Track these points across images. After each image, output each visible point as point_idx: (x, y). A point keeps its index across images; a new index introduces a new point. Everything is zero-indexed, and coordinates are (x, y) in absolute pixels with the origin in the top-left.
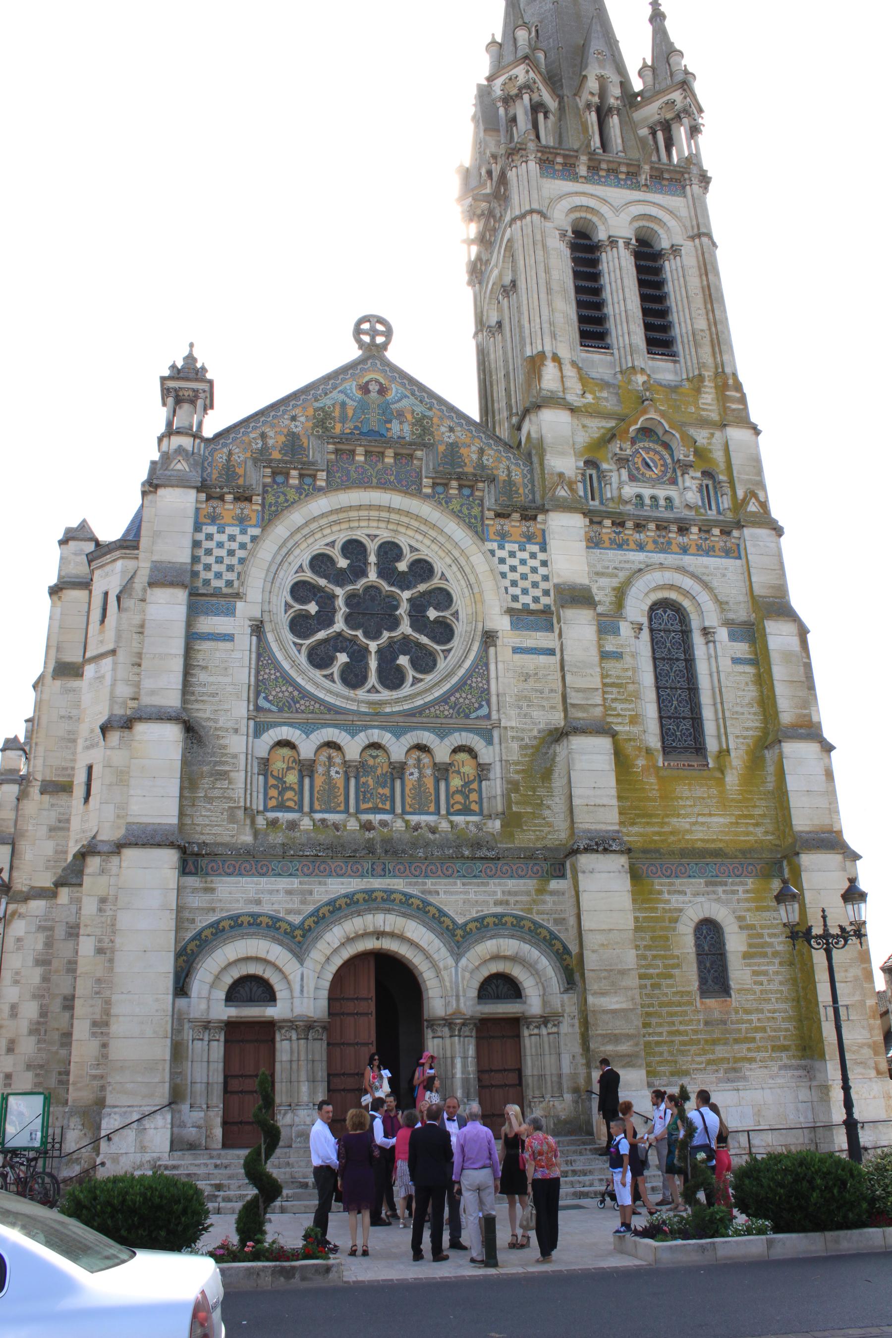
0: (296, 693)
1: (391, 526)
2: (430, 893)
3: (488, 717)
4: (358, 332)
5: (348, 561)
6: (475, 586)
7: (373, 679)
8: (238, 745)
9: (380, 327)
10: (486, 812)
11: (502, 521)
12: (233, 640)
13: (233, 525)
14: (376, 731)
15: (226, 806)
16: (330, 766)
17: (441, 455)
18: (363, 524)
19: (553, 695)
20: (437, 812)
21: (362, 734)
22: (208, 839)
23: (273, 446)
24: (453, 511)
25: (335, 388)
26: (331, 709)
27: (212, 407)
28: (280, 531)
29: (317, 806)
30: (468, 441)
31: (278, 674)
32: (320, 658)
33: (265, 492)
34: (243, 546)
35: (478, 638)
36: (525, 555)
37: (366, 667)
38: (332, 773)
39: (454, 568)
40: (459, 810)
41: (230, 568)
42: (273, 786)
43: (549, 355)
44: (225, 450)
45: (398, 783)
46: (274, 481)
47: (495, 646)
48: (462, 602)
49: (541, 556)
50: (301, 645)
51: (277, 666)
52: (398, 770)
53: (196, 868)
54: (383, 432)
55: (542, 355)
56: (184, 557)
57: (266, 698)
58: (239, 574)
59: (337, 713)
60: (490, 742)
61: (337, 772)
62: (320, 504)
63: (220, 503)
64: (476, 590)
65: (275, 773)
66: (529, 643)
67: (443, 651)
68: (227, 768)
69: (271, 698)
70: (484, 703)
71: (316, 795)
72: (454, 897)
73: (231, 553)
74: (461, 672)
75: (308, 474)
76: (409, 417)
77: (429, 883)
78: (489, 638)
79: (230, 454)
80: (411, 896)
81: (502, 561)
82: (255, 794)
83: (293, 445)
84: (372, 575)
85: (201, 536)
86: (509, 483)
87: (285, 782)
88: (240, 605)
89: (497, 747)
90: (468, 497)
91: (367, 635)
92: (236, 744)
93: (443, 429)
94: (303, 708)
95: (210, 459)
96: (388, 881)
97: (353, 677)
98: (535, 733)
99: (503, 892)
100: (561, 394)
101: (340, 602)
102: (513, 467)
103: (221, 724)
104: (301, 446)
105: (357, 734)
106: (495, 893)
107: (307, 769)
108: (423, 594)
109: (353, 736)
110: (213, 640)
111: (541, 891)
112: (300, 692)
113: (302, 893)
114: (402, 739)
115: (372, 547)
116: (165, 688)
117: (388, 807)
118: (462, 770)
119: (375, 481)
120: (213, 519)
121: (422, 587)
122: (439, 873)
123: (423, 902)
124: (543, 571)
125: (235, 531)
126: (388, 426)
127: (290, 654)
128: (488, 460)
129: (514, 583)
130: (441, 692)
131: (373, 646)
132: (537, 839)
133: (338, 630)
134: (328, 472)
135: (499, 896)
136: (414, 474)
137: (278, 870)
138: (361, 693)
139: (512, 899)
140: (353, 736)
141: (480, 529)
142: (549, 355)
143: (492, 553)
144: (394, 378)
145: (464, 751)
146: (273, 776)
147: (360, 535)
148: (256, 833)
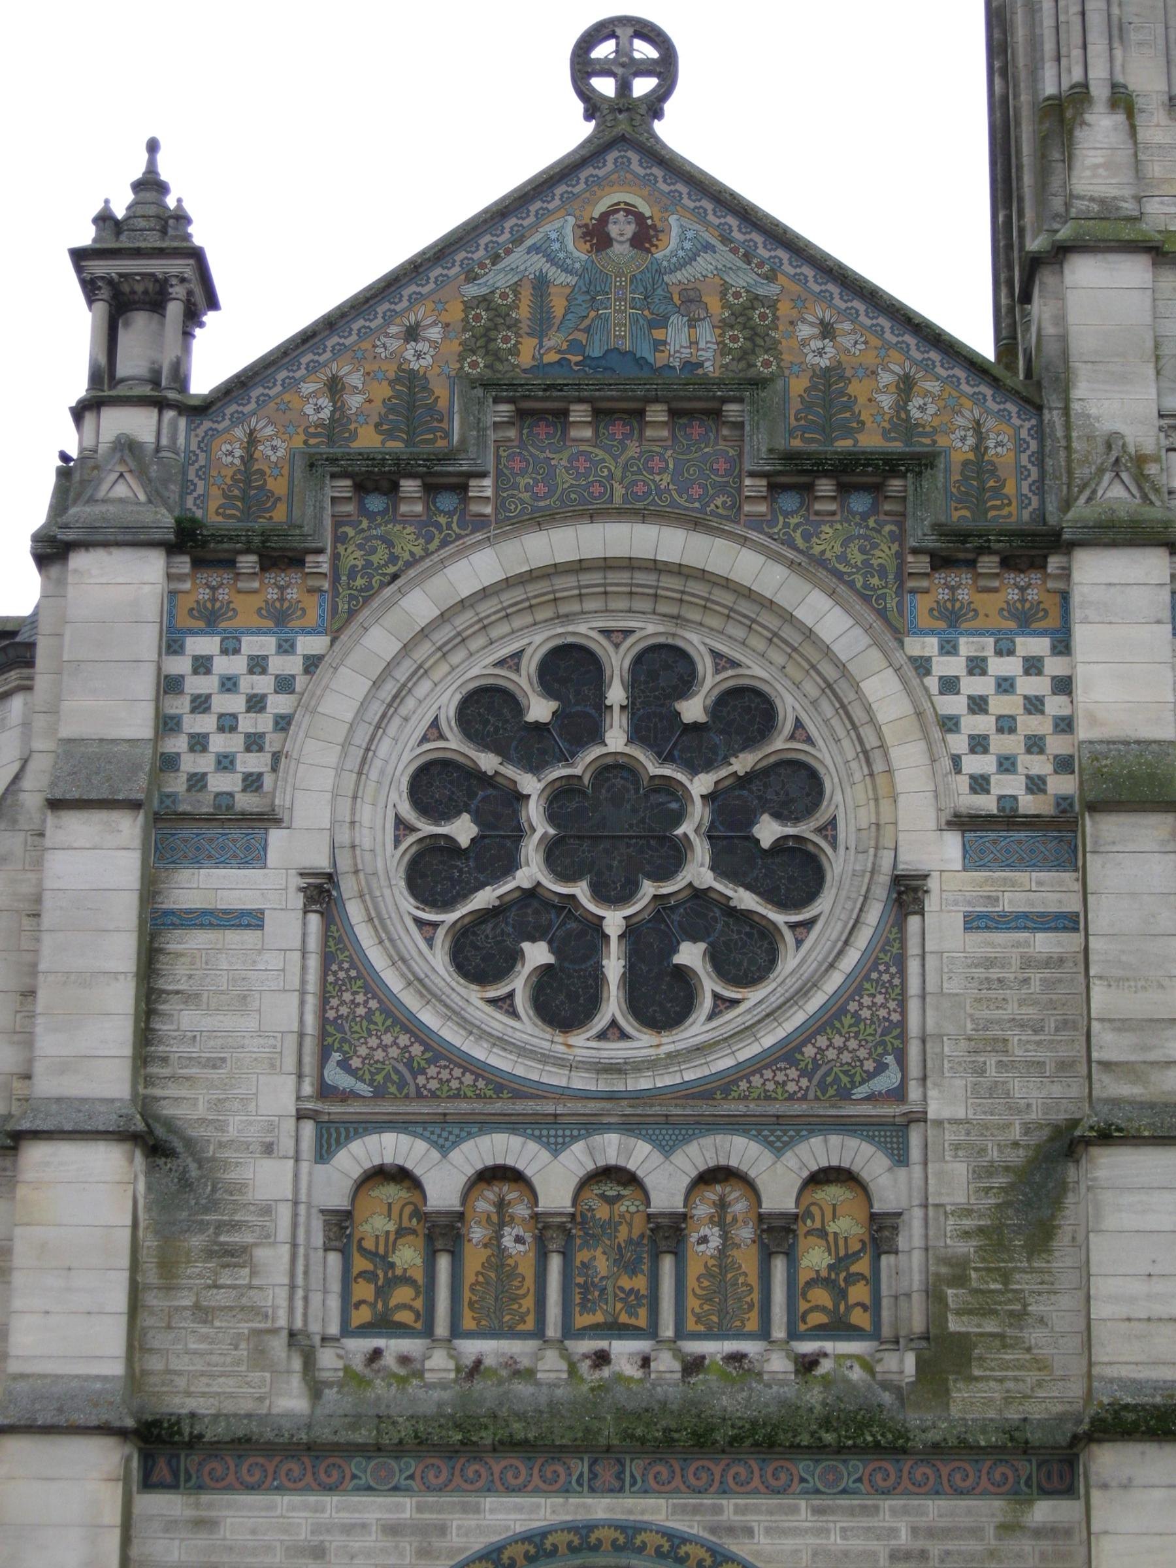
0: (417, 1050)
1: (663, 608)
2: (731, 1530)
3: (899, 1094)
4: (582, 67)
5: (553, 705)
6: (877, 756)
7: (613, 1005)
8: (279, 1181)
9: (644, 50)
10: (886, 1331)
11: (953, 577)
12: (260, 927)
13: (259, 632)
14: (613, 1139)
15: (245, 1327)
16: (502, 1224)
17: (795, 405)
18: (590, 605)
19: (1065, 1035)
20: (764, 1333)
21: (578, 1148)
22: (203, 1406)
23: (360, 412)
24: (820, 562)
25: (518, 241)
26: (503, 1085)
27: (213, 303)
28: (378, 640)
29: (468, 1323)
30: (870, 359)
31: (373, 1004)
32: (480, 955)
33: (340, 539)
34: (285, 684)
35: (881, 891)
36: (1010, 666)
37: (598, 978)
38: (508, 1241)
39: (827, 709)
40: (821, 1327)
41: (254, 743)
42: (361, 1274)
43: (1100, 92)
44: (239, 432)
45: (667, 1264)
46: (363, 511)
47: (922, 913)
48: (846, 799)
49: (1055, 666)
50: (435, 925)
51: (370, 983)
52: (669, 1233)
53: (175, 1474)
54: (645, 351)
55: (1080, 95)
56: (135, 723)
57: (344, 1065)
58: (276, 757)
59: (517, 1095)
60: (901, 1158)
61: (519, 1240)
62: (478, 568)
63: (227, 576)
64: (879, 767)
65: (369, 1244)
66: (1011, 902)
67: (793, 926)
68: (249, 1239)
69: (355, 1063)
70: (889, 1059)
71: (467, 1295)
72: (789, 1543)
73: (256, 703)
74: (834, 981)
75: (446, 482)
76: (714, 303)
77: (730, 1508)
78: (907, 892)
79: (252, 440)
80: (685, 1540)
81: (949, 685)
82: (316, 1298)
83: (411, 406)
84: (616, 739)
85: (179, 665)
86: (980, 466)
87: (392, 1265)
88: (276, 837)
89: (917, 1170)
90: (865, 517)
91: (601, 893)
92: (268, 1180)
93: (805, 331)
94: (434, 1085)
95: (202, 456)
96: (629, 1502)
97: (565, 1001)
98: (1016, 1133)
99: (915, 1531)
100: (1129, 207)
101: (534, 812)
102: (990, 423)
103: (232, 1132)
104: (431, 408)
105: (565, 1145)
106: (893, 1532)
107: (444, 1233)
108: (743, 781)
109: (556, 1150)
110: (211, 926)
111: (1007, 1529)
112: (427, 1048)
113: (423, 1530)
114: (679, 1158)
115: (617, 662)
116: (88, 1054)
117: (642, 1321)
118: (832, 1228)
119: (619, 490)
120: (210, 618)
121: (743, 763)
122: (756, 1482)
123: (713, 1551)
124: (1055, 706)
125: (266, 645)
126: (658, 334)
127: (405, 951)
128: (921, 410)
129: (979, 744)
130: (780, 1034)
131: (614, 921)
132: (1008, 1400)
133: (526, 885)
134: (499, 474)
135: (904, 1539)
136: (721, 466)
137: (367, 1479)
138: (581, 1043)
139: (935, 1548)
140: (556, 1150)
141: (892, 604)
142: (1100, 92)
143: (922, 666)
144: (675, 199)
145: (828, 1182)
146: (362, 1250)
147: (584, 630)
148: (316, 1389)
